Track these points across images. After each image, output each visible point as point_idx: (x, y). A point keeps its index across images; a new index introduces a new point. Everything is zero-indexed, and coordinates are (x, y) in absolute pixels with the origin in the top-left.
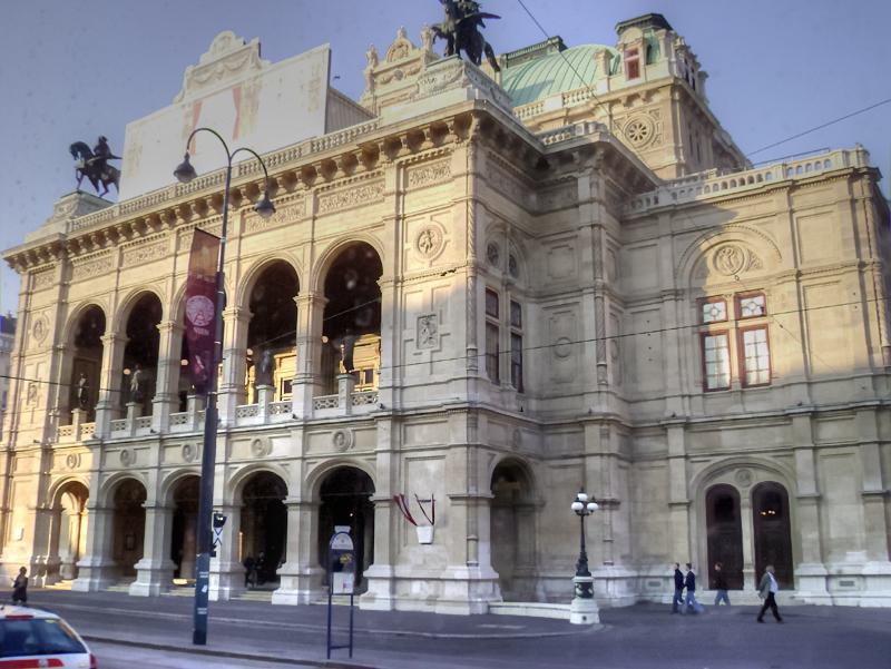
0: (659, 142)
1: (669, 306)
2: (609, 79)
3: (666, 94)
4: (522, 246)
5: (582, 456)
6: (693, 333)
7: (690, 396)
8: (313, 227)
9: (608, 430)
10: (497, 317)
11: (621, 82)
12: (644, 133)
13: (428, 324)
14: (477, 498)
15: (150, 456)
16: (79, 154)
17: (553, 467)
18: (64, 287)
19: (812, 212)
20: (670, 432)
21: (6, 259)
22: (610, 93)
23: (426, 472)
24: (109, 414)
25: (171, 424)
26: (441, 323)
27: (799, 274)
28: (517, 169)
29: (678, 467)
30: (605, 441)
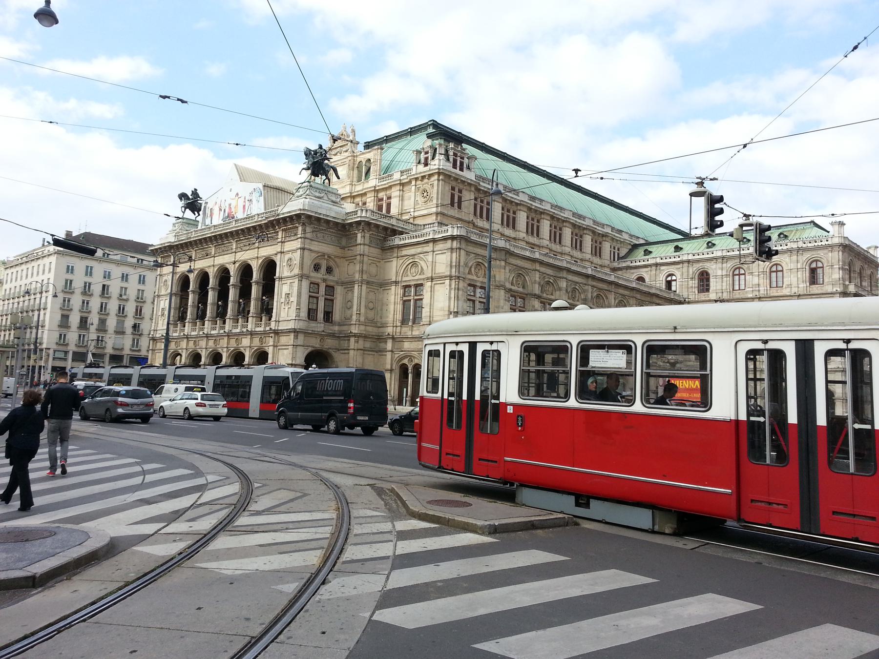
0: (432, 201)
1: (393, 288)
2: (417, 166)
3: (436, 177)
4: (335, 262)
5: (349, 350)
7: (396, 327)
8: (258, 251)
9: (358, 340)
10: (318, 293)
11: (421, 168)
12: (427, 195)
13: (288, 297)
15: (203, 343)
16: (183, 198)
17: (342, 353)
18: (174, 265)
19: (440, 252)
20: (388, 341)
22: (416, 174)
23: (283, 354)
24: (190, 324)
25: (211, 330)
27: (432, 279)
28: (331, 230)
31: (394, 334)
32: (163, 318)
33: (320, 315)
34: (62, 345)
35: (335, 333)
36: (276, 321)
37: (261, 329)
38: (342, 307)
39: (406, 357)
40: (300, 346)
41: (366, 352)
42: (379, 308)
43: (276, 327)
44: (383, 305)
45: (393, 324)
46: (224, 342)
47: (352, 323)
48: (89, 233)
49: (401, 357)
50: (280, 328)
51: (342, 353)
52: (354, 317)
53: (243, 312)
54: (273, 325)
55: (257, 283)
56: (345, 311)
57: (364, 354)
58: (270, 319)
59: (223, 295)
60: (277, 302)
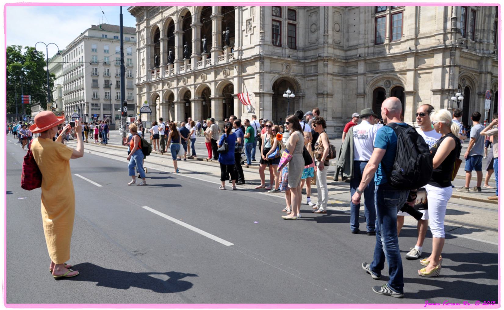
5: (317, 76)
6: (372, 17)
10: (281, 17)
14: (263, 93)
17: (309, 80)
20: (359, 63)
21: (130, 12)
26: (253, 22)
29: (361, 79)
30: (326, 69)
31: (366, 55)
32: (144, 67)
33: (285, 40)
34: (96, 99)
35: (299, 60)
36: (238, 50)
37: (224, 61)
38: (306, 32)
39: (383, 79)
40: (266, 72)
41: (335, 78)
42: (345, 31)
43: (240, 57)
44: (349, 26)
45: (365, 44)
46: (191, 81)
47: (321, 45)
48: (105, 24)
49: (375, 80)
50: (243, 57)
51: (309, 80)
52: (322, 40)
53: (206, 49)
54: (236, 55)
55: (215, 17)
56: (309, 36)
57: (333, 79)
58: (232, 48)
59: (187, 39)
60: (239, 30)
